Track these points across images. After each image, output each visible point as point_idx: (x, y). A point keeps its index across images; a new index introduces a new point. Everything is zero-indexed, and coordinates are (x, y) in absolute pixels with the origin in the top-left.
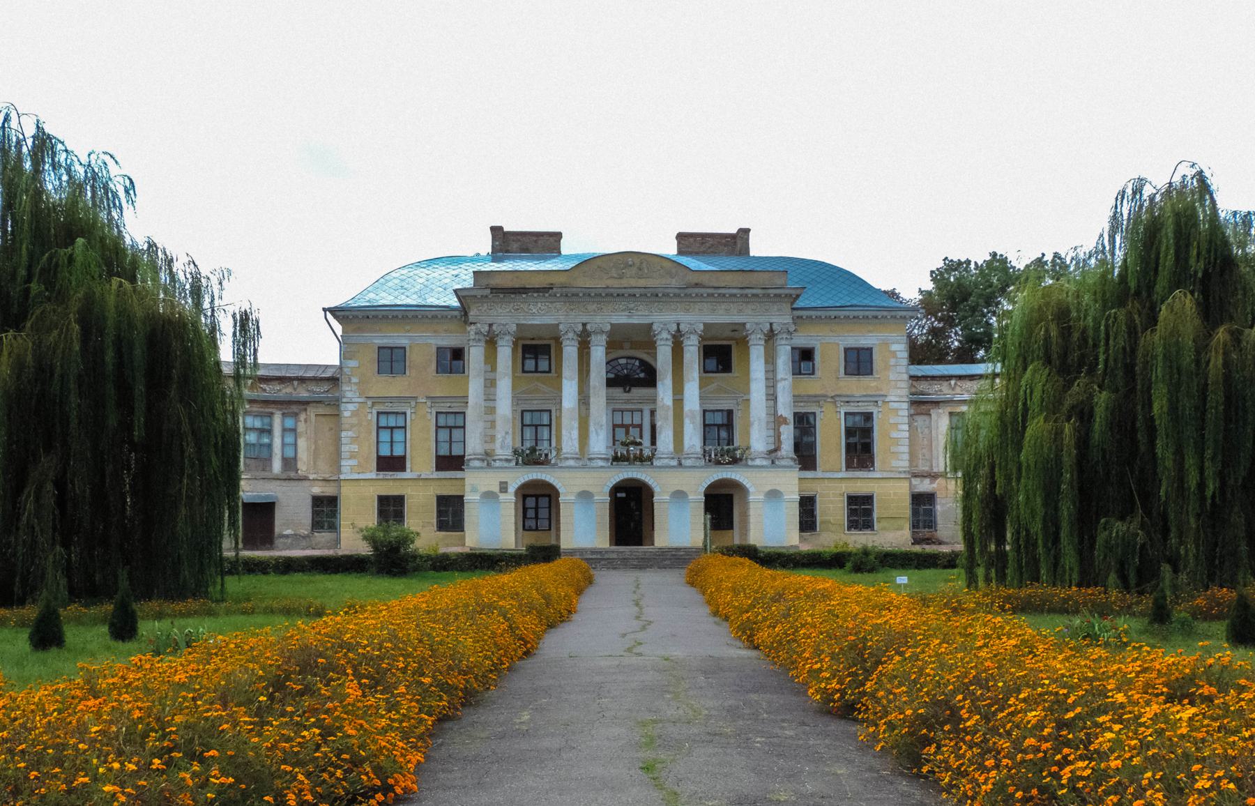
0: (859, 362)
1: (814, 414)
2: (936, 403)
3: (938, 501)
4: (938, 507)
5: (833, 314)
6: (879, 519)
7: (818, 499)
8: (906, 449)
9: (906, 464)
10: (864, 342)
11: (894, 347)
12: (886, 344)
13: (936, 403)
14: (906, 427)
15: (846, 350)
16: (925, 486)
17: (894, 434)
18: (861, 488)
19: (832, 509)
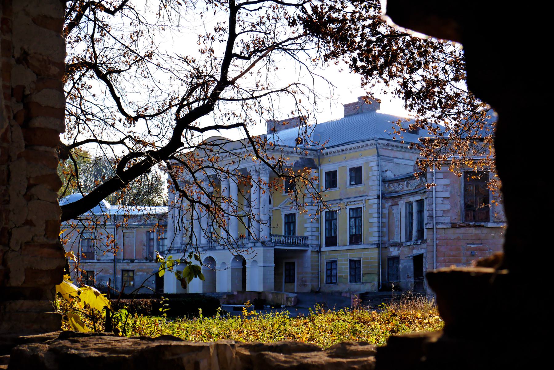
0: (356, 175)
1: (361, 208)
2: (400, 197)
3: (401, 262)
4: (401, 266)
5: (340, 148)
6: (364, 275)
7: (338, 263)
8: (376, 229)
9: (376, 239)
10: (356, 164)
11: (372, 164)
12: (368, 163)
13: (400, 197)
14: (376, 215)
15: (351, 170)
16: (394, 252)
17: (371, 220)
18: (356, 256)
19: (343, 269)
